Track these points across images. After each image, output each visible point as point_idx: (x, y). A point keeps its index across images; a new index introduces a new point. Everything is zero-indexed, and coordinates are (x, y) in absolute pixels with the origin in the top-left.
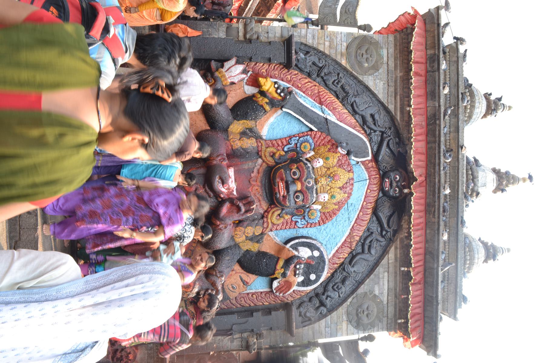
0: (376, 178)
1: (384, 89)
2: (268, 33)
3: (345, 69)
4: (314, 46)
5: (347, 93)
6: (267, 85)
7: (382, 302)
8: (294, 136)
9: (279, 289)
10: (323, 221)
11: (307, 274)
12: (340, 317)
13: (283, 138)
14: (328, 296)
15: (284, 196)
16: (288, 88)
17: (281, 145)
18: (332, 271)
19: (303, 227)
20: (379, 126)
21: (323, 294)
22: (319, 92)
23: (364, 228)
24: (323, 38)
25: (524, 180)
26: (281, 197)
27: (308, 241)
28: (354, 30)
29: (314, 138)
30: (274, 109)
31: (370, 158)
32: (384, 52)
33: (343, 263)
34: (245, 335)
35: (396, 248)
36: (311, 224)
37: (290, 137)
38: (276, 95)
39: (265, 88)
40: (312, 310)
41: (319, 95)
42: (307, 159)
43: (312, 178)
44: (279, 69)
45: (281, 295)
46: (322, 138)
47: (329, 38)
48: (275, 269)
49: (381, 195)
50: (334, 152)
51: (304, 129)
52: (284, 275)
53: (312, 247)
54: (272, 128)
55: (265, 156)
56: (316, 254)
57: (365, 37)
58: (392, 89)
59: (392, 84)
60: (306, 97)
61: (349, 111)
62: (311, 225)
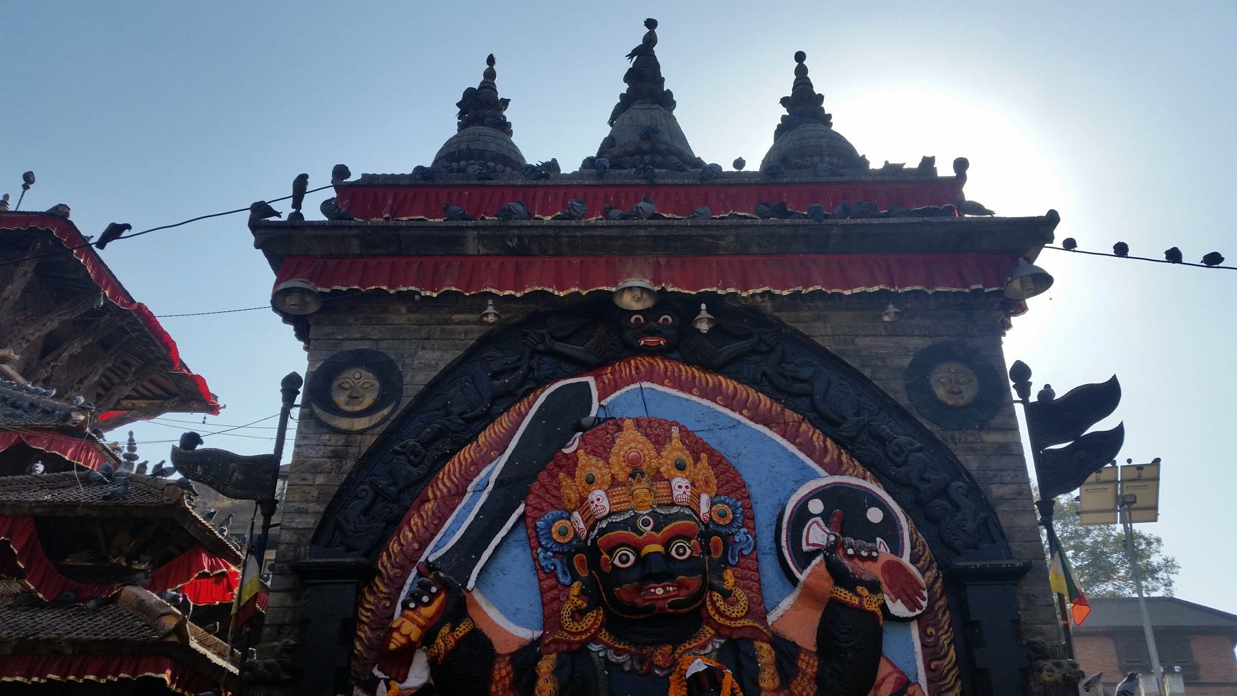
0: (637, 368)
1: (433, 349)
2: (281, 626)
4: (322, 509)
5: (441, 434)
6: (407, 627)
8: (536, 560)
10: (738, 489)
11: (870, 532)
12: (973, 449)
13: (540, 587)
14: (922, 479)
15: (680, 586)
16: (420, 574)
17: (555, 592)
18: (861, 469)
19: (755, 538)
20: (519, 360)
21: (917, 489)
22: (435, 498)
23: (752, 391)
24: (307, 489)
26: (684, 592)
27: (784, 525)
29: (542, 510)
30: (471, 611)
31: (591, 380)
32: (349, 346)
33: (836, 441)
36: (746, 517)
37: (538, 568)
38: (437, 603)
39: (415, 634)
40: (959, 515)
41: (442, 497)
42: (592, 528)
43: (636, 516)
44: (371, 598)
45: (925, 594)
46: (541, 492)
47: (307, 476)
48: (860, 610)
49: (676, 355)
50: (576, 465)
51: (522, 534)
52: (874, 587)
53: (802, 515)
54: (513, 616)
55: (581, 633)
56: (816, 506)
59: (425, 331)
60: (443, 530)
61: (484, 429)
62: (749, 518)
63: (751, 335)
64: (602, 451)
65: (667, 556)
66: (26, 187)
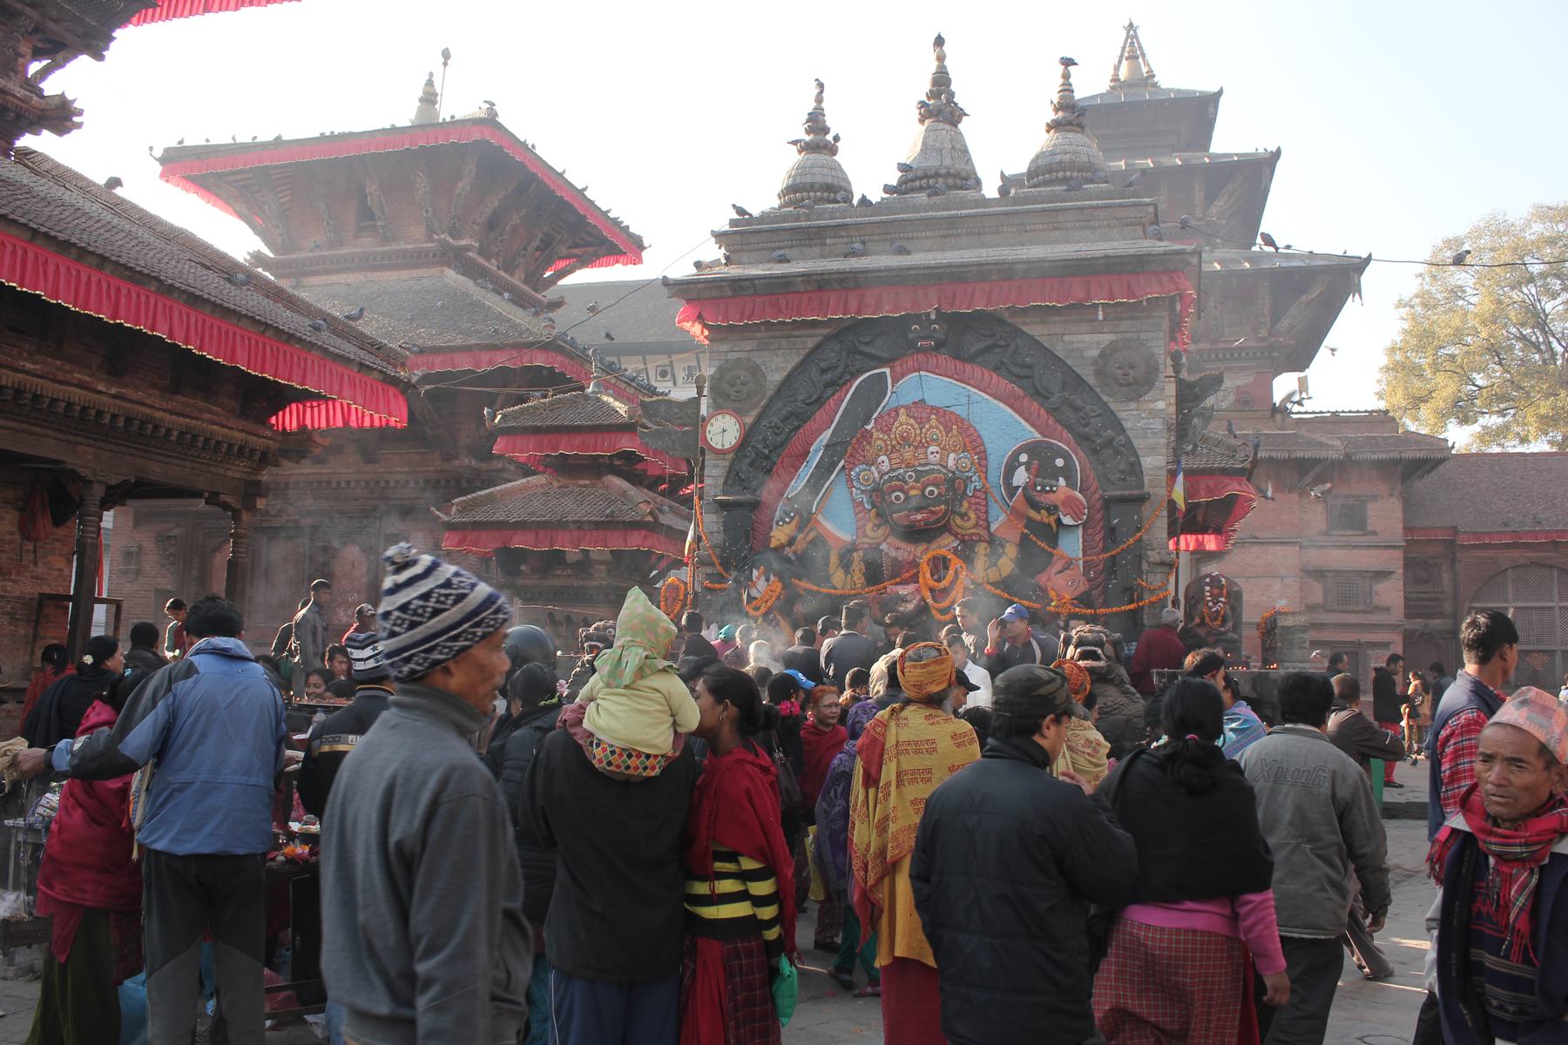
3: (759, 417)
5: (792, 414)
7: (1112, 342)
9: (1076, 516)
25: (941, 58)
28: (704, 401)
31: (887, 370)
33: (1048, 412)
34: (1145, 566)
35: (1025, 324)
37: (854, 500)
38: (794, 523)
48: (1041, 523)
51: (843, 479)
52: (1052, 509)
56: (1024, 458)
57: (712, 389)
58: (784, 342)
63: (993, 336)
64: (887, 430)
65: (923, 495)
66: (445, 64)
